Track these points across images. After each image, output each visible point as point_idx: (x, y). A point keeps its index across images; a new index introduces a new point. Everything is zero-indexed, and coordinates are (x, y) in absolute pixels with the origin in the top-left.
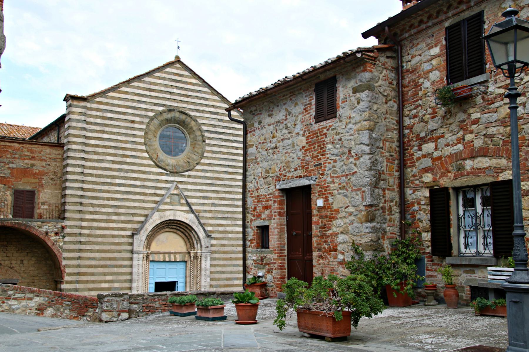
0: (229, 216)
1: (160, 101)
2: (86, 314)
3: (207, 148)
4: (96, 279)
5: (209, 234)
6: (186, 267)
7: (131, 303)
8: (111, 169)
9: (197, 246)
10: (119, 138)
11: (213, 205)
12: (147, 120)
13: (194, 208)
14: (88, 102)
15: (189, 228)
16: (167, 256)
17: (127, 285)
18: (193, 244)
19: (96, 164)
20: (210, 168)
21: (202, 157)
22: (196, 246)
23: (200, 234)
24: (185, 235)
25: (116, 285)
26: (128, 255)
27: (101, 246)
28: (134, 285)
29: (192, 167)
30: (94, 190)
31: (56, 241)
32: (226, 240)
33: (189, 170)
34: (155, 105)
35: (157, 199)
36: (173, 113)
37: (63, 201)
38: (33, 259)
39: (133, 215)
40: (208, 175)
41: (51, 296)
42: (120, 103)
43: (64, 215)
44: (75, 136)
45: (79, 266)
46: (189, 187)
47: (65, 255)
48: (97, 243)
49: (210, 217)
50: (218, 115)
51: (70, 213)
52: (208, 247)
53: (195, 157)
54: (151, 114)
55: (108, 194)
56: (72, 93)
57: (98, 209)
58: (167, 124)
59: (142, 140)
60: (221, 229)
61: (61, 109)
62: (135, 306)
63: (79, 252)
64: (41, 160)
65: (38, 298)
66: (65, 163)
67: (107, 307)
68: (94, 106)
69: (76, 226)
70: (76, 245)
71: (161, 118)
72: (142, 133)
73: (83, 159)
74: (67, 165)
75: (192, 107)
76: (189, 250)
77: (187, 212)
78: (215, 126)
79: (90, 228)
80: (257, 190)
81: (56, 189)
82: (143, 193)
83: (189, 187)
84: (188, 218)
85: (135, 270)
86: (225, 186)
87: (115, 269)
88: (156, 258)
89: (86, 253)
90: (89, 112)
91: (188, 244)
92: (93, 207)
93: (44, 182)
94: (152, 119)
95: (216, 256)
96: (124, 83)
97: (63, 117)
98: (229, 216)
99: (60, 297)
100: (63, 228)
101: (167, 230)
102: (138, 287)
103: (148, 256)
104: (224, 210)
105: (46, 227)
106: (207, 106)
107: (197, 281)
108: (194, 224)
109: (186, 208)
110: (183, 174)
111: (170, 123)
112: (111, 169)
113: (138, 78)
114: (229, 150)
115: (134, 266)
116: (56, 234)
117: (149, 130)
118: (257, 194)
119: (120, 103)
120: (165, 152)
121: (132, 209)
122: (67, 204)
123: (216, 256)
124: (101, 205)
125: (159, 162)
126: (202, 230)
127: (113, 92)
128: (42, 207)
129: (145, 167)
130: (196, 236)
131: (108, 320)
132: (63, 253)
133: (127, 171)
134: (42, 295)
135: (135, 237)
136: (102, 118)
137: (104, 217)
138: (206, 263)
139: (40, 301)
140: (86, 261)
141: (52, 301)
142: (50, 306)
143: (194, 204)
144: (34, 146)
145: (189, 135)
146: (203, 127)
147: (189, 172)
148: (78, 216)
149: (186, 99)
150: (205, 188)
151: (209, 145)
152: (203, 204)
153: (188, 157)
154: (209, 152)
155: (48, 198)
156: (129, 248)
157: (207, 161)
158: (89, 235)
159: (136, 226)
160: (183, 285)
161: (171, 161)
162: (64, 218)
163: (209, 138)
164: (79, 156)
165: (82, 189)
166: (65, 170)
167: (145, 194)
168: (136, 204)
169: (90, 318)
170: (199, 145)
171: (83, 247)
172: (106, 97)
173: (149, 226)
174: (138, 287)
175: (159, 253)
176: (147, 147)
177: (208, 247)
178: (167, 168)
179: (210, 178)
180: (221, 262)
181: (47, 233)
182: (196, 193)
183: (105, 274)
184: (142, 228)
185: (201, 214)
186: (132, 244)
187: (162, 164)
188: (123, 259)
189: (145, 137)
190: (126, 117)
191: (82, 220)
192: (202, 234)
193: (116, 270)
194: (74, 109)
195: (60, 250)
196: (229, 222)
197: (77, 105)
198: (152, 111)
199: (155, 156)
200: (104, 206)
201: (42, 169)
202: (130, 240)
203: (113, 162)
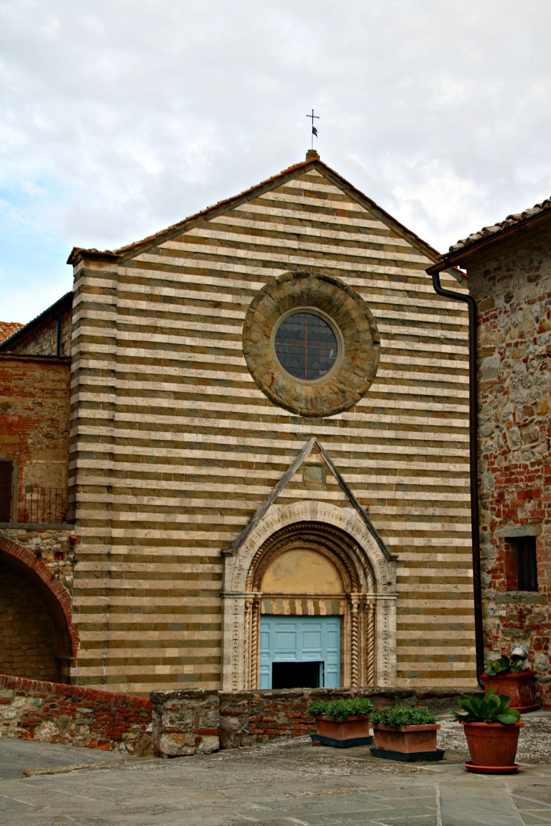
0: (438, 511)
1: (275, 255)
2: (124, 735)
3: (385, 358)
4: (145, 655)
5: (393, 554)
6: (342, 628)
7: (224, 714)
8: (172, 411)
9: (366, 582)
10: (188, 341)
11: (399, 487)
12: (247, 300)
13: (357, 494)
14: (121, 264)
15: (346, 539)
17: (211, 669)
18: (357, 576)
19: (140, 401)
20: (391, 404)
21: (373, 378)
22: (362, 582)
24: (338, 555)
25: (188, 669)
26: (213, 602)
27: (153, 582)
28: (228, 669)
29: (350, 402)
30: (137, 459)
31: (58, 572)
32: (431, 567)
33: (344, 410)
34: (264, 266)
35: (275, 475)
36: (305, 281)
37: (71, 482)
38: (10, 611)
39: (223, 511)
40: (387, 419)
41: (49, 696)
42: (189, 263)
43: (74, 515)
44: (94, 340)
45: (107, 627)
46: (345, 447)
47: (78, 601)
48: (145, 576)
50: (406, 282)
51: (87, 509)
52: (389, 584)
53: (356, 380)
54: (257, 286)
56: (86, 246)
57: (145, 500)
58: (293, 307)
59: (239, 346)
60: (419, 542)
61: (63, 283)
62: (234, 721)
63: (107, 595)
64: (24, 394)
65: (23, 699)
66: (73, 400)
67: (172, 722)
68: (133, 272)
69: (100, 538)
70: (100, 580)
71: (278, 294)
72: (238, 330)
73: (113, 389)
74: (80, 404)
75: (348, 266)
76: (349, 590)
78: (400, 307)
79: (130, 541)
80: (504, 453)
81: (56, 457)
82: (243, 462)
83: (345, 447)
84: (344, 518)
85: (228, 635)
86: (426, 443)
87: (186, 633)
88: (274, 607)
89: (122, 598)
90: (124, 287)
91: (345, 576)
92: (136, 495)
93: (30, 441)
94: (258, 296)
95: (410, 603)
96: (196, 217)
97: (69, 297)
98: (438, 511)
99: (68, 697)
100: (73, 542)
101: (298, 544)
102: (235, 675)
103: (256, 603)
104: (424, 498)
105: (36, 541)
106: (381, 262)
107: (366, 661)
108: (359, 530)
110: (331, 418)
111: (299, 305)
112: (172, 411)
113: (227, 206)
114: (434, 360)
115: (225, 627)
116: (59, 555)
117: (254, 322)
118: (505, 464)
119: (189, 263)
120: (289, 369)
121: (220, 498)
122: (80, 489)
123: (410, 603)
124: (154, 490)
125: (276, 392)
127: (172, 239)
128: (28, 497)
129: (245, 403)
130: (363, 560)
131: (175, 753)
132: (74, 598)
133: (206, 414)
134: (31, 692)
135: (227, 560)
136: (151, 298)
137: (160, 518)
138: (387, 621)
139: (28, 707)
140: (122, 615)
141: (53, 706)
142: (48, 718)
143: (358, 486)
144: (7, 364)
145: (343, 330)
146: (372, 311)
147: (345, 413)
148: (103, 515)
149: (334, 249)
150: (380, 449)
152: (378, 486)
153: (341, 379)
155: (40, 478)
156: (215, 585)
157: (384, 388)
158: (127, 558)
159: (228, 536)
160: (336, 670)
161: (303, 389)
162: (74, 521)
163: (388, 336)
164: (104, 384)
165: (112, 456)
166: (74, 416)
167: (248, 465)
168: (229, 488)
169: (134, 745)
170: (365, 351)
171: (115, 583)
172: (157, 253)
173: (258, 537)
174: (235, 675)
175: (280, 596)
176: (250, 359)
177: (389, 584)
178: (295, 405)
179: (391, 426)
180: (422, 619)
181: (38, 553)
182: (360, 461)
183: (163, 644)
184: (241, 541)
185: (374, 509)
186: (220, 577)
187: (283, 397)
188: (203, 610)
189: (245, 338)
191: (112, 523)
192: (375, 555)
193: (186, 635)
194: (92, 282)
195: (68, 591)
196: (438, 526)
197: (96, 272)
198: (258, 278)
200: (159, 493)
201: (25, 414)
202: (217, 569)
203: (178, 395)
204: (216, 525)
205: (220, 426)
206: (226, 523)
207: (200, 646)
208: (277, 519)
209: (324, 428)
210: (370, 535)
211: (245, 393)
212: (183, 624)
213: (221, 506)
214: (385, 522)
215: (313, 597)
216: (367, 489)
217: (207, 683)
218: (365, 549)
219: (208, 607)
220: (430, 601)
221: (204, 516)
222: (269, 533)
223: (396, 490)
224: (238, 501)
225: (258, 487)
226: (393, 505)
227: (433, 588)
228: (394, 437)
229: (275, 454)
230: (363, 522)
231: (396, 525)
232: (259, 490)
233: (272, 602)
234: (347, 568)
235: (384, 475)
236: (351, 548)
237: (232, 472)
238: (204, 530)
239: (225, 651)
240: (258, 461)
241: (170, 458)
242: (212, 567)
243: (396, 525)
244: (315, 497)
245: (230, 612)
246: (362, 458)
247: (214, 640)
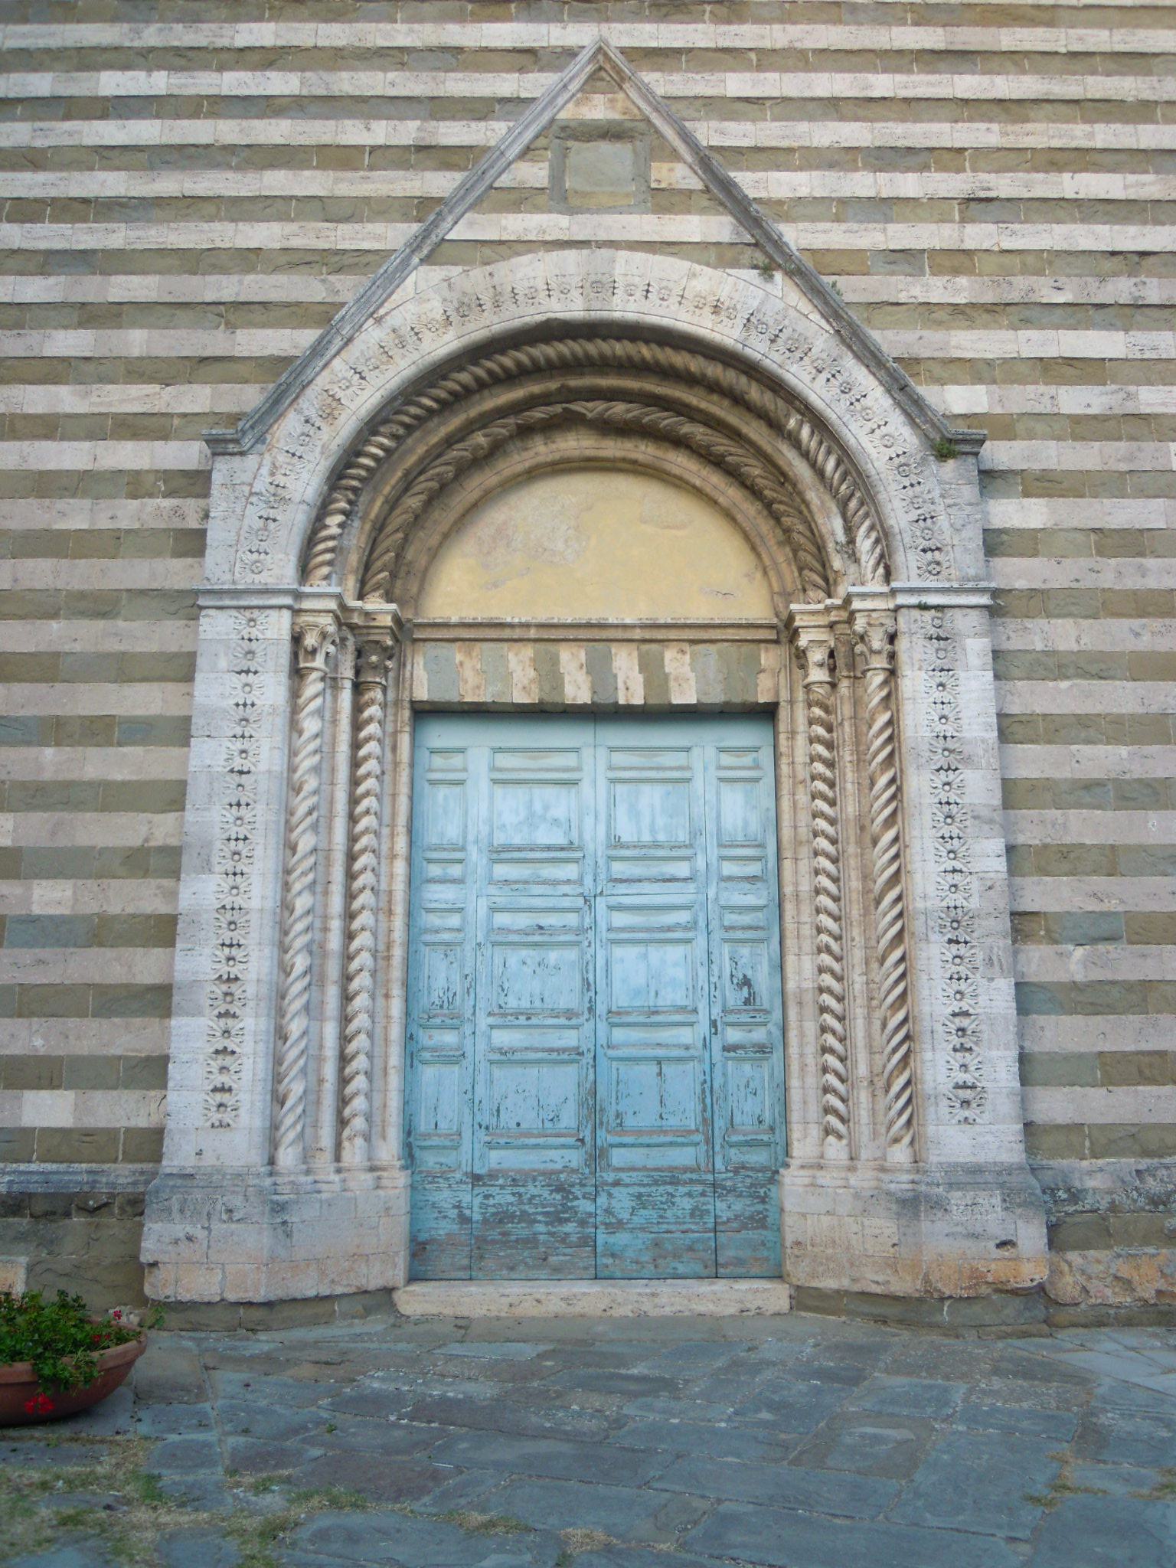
11: (975, 206)
15: (755, 393)
23: (856, 434)
24: (733, 473)
32: (1142, 493)
46: (737, 84)
49: (956, 309)
55: (28, 177)
77: (719, 255)
83: (737, 84)
87: (49, 752)
102: (232, 915)
108: (798, 349)
115: (198, 722)
121: (224, 270)
126: (878, 398)
138: (950, 697)
150: (882, 84)
152: (884, 208)
159: (250, 397)
173: (359, 383)
182: (803, 127)
192: (877, 431)
204: (203, 360)
205: (240, 42)
206: (238, 352)
207: (105, 808)
208: (438, 315)
209: (649, 28)
210: (849, 362)
212: (43, 720)
213: (227, 295)
214: (926, 333)
215: (638, 634)
216: (837, 219)
217: (127, 952)
218: (831, 415)
219: (153, 656)
220: (1156, 624)
221: (156, 333)
222: (403, 368)
223: (963, 221)
224: (296, 278)
225: (378, 228)
226: (956, 272)
228: (942, 46)
229: (453, 118)
230: (815, 316)
232: (378, 238)
233: (459, 657)
234: (776, 518)
235: (908, 170)
236: (775, 426)
237: (277, 182)
238: (151, 380)
239: (190, 816)
240: (381, 141)
241: (43, 151)
242: (175, 511)
244: (602, 236)
245: (223, 664)
246: (811, 119)
247: (167, 782)
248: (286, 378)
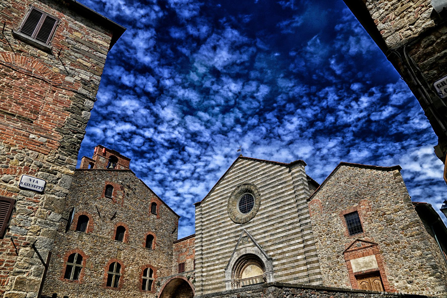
3: (262, 198)
12: (227, 199)
16: (251, 281)
21: (260, 205)
54: (229, 194)
60: (279, 251)
71: (235, 194)
77: (253, 246)
94: (230, 197)
108: (259, 252)
109: (252, 244)
126: (264, 256)
150: (264, 225)
151: (263, 196)
152: (265, 237)
154: (263, 200)
162: (195, 269)
163: (263, 191)
167: (230, 243)
168: (227, 251)
173: (232, 263)
178: (240, 221)
190: (219, 203)
198: (229, 192)
199: (234, 217)
203: (215, 230)
211: (229, 223)
227: (286, 266)
231: (271, 248)
237: (227, 246)
243: (271, 248)
248: (229, 261)
